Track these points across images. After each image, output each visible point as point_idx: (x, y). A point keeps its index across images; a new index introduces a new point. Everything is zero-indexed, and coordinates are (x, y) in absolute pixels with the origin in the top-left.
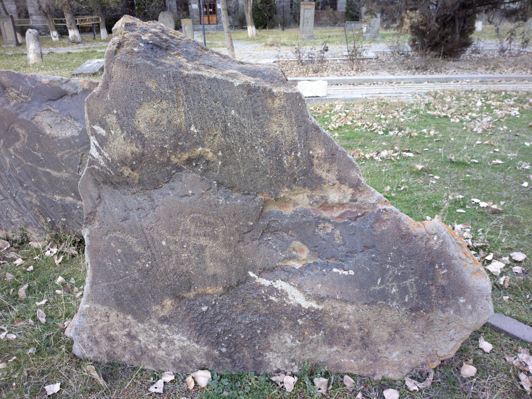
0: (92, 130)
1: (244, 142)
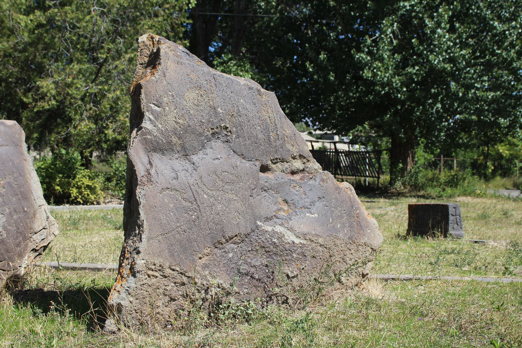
0: (148, 107)
1: (249, 121)
